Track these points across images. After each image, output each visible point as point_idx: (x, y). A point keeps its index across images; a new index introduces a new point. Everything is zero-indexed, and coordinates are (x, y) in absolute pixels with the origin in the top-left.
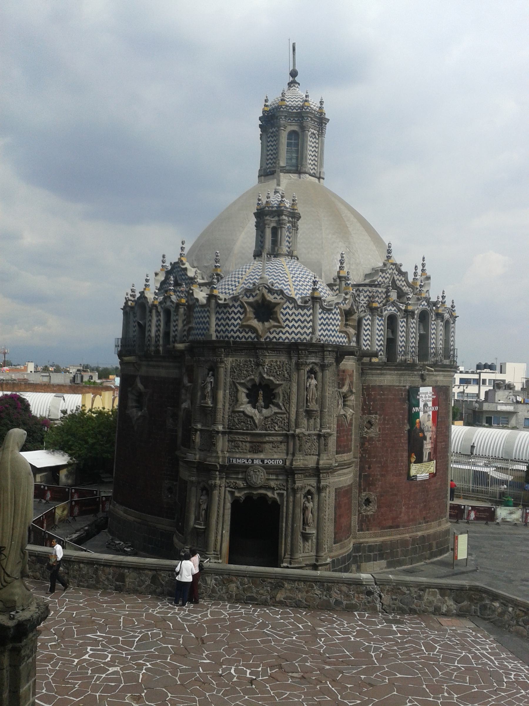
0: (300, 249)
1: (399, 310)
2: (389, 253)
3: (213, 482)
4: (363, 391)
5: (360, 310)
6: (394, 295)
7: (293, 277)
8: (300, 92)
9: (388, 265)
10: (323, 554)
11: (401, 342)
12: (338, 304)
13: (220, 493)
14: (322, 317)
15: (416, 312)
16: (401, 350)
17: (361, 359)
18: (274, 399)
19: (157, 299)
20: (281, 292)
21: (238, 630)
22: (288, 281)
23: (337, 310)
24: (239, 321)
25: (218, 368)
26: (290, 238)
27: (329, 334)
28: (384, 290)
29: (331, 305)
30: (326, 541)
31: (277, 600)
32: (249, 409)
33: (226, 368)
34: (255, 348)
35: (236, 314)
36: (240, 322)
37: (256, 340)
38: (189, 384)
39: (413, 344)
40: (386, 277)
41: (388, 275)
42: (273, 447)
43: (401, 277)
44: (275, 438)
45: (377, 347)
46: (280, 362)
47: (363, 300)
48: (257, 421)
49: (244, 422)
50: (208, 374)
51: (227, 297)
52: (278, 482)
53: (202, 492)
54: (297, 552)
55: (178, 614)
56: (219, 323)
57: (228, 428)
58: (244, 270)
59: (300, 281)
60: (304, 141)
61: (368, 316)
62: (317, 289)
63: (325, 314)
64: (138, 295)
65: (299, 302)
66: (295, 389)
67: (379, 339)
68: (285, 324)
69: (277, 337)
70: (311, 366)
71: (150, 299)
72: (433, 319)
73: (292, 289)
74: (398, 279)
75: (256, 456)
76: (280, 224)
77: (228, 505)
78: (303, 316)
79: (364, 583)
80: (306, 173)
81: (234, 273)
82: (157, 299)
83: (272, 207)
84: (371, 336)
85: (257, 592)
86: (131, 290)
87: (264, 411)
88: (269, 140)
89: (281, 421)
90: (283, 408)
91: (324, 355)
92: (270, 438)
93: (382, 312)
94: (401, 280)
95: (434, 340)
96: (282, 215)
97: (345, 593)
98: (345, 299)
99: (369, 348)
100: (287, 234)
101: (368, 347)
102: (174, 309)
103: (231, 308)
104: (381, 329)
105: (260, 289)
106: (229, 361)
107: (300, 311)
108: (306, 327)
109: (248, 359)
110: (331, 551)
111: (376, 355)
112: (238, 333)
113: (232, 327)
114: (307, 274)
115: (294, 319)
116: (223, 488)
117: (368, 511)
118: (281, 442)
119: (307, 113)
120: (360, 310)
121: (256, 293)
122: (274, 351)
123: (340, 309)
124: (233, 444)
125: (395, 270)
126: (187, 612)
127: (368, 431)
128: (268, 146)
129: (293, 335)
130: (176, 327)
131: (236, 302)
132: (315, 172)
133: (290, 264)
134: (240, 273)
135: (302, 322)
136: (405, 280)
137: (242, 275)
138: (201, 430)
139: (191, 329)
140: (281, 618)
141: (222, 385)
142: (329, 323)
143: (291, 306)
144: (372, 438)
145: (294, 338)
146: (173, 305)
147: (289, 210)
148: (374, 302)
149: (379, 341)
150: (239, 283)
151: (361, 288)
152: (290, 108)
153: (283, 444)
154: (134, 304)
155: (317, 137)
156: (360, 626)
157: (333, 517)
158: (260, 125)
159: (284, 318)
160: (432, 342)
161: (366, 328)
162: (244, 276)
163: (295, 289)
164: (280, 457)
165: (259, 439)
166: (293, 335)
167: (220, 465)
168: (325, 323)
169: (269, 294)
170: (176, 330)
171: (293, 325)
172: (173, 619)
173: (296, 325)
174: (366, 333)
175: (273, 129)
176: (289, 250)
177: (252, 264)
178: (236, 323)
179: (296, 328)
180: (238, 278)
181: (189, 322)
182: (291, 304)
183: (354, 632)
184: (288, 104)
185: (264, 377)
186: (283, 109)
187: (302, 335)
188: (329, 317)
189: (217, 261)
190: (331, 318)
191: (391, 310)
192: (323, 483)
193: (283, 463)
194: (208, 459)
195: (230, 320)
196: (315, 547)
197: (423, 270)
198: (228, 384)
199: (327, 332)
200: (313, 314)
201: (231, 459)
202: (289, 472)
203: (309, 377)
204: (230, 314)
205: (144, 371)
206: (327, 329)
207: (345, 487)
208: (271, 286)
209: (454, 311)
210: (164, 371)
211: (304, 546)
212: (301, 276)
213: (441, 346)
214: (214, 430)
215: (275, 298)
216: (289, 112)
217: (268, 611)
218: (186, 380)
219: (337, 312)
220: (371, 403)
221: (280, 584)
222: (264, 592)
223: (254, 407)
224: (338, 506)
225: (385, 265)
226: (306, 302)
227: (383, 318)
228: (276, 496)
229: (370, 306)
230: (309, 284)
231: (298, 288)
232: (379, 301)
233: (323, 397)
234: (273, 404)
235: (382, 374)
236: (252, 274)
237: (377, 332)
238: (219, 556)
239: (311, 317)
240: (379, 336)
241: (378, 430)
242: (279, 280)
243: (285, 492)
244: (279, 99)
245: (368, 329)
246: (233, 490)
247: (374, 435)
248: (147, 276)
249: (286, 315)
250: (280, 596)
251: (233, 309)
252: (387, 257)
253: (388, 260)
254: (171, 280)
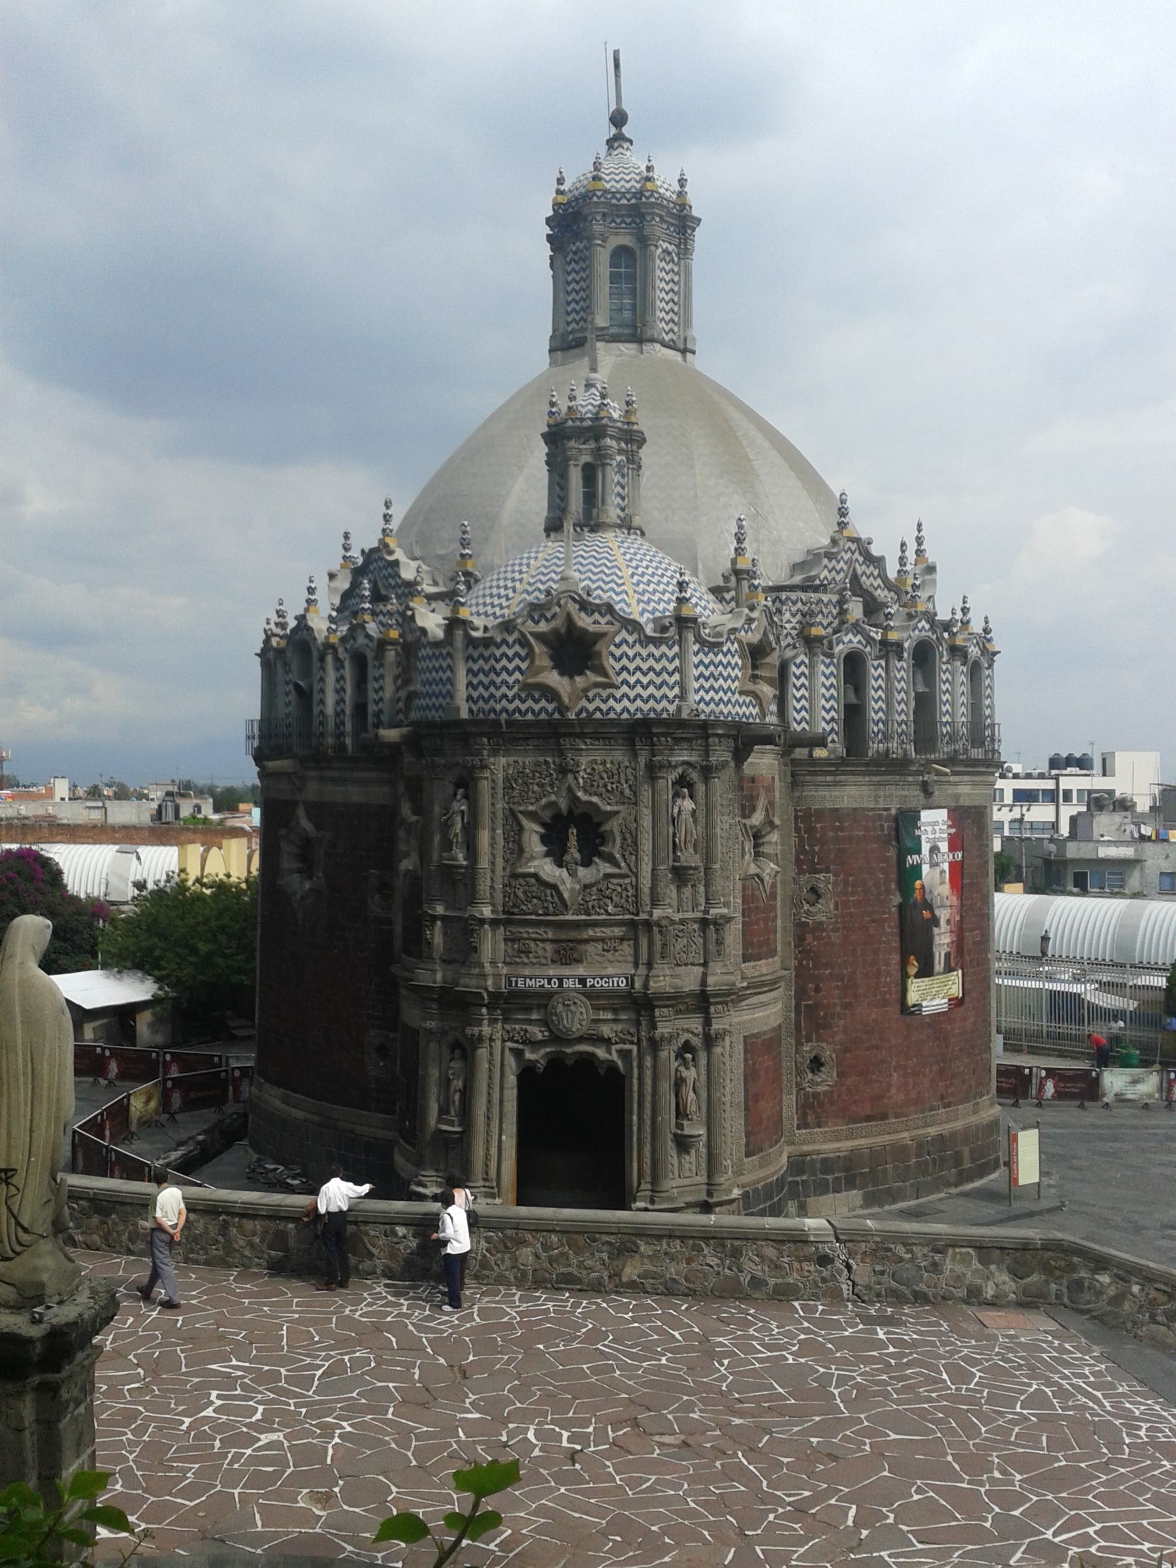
0: (648, 511)
1: (870, 640)
2: (843, 515)
3: (476, 1030)
4: (796, 823)
5: (783, 644)
6: (856, 610)
7: (633, 575)
8: (635, 159)
9: (841, 543)
10: (722, 1180)
11: (876, 713)
12: (734, 630)
13: (491, 1054)
14: (701, 662)
15: (906, 645)
16: (876, 729)
17: (791, 753)
18: (602, 844)
19: (335, 631)
20: (609, 609)
21: (541, 1347)
22: (623, 584)
23: (733, 643)
24: (517, 675)
25: (476, 780)
26: (623, 487)
27: (717, 698)
28: (835, 598)
29: (720, 635)
30: (729, 1151)
31: (624, 1279)
32: (548, 869)
33: (493, 781)
34: (556, 734)
35: (510, 660)
36: (520, 678)
37: (556, 716)
38: (414, 818)
39: (903, 717)
40: (838, 568)
41: (842, 563)
42: (604, 950)
43: (871, 568)
44: (608, 932)
45: (824, 724)
46: (612, 762)
47: (790, 621)
48: (566, 895)
49: (539, 899)
50: (455, 794)
51: (491, 622)
52: (619, 1027)
53: (452, 1052)
54: (666, 1177)
55: (408, 1316)
56: (475, 681)
57: (504, 912)
58: (525, 561)
59: (649, 583)
60: (647, 272)
61: (802, 657)
62: (688, 600)
63: (706, 654)
64: (292, 624)
65: (649, 630)
66: (646, 822)
67: (828, 706)
68: (620, 679)
69: (604, 707)
70: (680, 770)
71: (320, 631)
72: (944, 660)
73: (634, 602)
74: (864, 573)
75: (566, 971)
76: (601, 455)
77: (512, 1080)
78: (658, 660)
79: (812, 1239)
80: (652, 340)
81: (503, 569)
82: (335, 631)
83: (582, 420)
84: (810, 700)
85: (581, 1265)
86: (277, 612)
87: (582, 871)
88: (569, 269)
89: (620, 894)
90: (623, 864)
91: (707, 746)
92: (597, 930)
93: (831, 648)
94: (872, 574)
95: (948, 706)
96: (605, 436)
97: (771, 1261)
98: (750, 620)
99: (807, 728)
100: (617, 478)
101: (804, 724)
102: (373, 654)
103: (498, 646)
104: (832, 685)
105: (562, 602)
106: (500, 765)
107: (652, 648)
108: (667, 684)
109: (541, 759)
110: (739, 1172)
111: (821, 742)
112: (517, 702)
113: (504, 689)
114: (663, 566)
115: (638, 668)
116: (499, 1043)
117: (818, 1084)
118: (622, 939)
119: (653, 205)
120: (783, 644)
121: (553, 612)
122: (598, 739)
123: (740, 642)
124: (516, 946)
125: (857, 554)
126: (428, 1312)
127: (811, 909)
128: (568, 283)
129: (639, 703)
130: (381, 693)
131: (510, 633)
132: (675, 338)
133: (626, 545)
134: (517, 568)
135: (658, 674)
136: (879, 575)
137: (521, 572)
138: (444, 918)
139: (412, 696)
140: (634, 1320)
141: (485, 818)
142: (716, 674)
143: (631, 639)
144: (821, 923)
145: (642, 710)
146: (370, 644)
147: (619, 424)
148: (813, 625)
149: (828, 711)
150: (514, 591)
151: (784, 595)
152: (614, 197)
153: (625, 943)
154: (283, 643)
155: (676, 259)
156: (806, 1331)
157: (741, 1098)
158: (548, 236)
159: (618, 666)
160: (944, 710)
161: (798, 684)
162: (524, 576)
163: (639, 601)
164: (620, 972)
165: (573, 935)
166: (639, 703)
167: (489, 993)
168: (707, 674)
169: (583, 614)
170: (381, 699)
171: (638, 681)
172: (398, 1328)
173: (645, 680)
174: (798, 695)
175: (578, 244)
176: (622, 515)
177: (541, 549)
178: (511, 680)
179: (645, 687)
180: (513, 580)
181: (408, 681)
182: (631, 634)
183: (794, 1345)
184: (608, 186)
185: (578, 798)
186: (599, 197)
187: (658, 701)
188: (717, 661)
189: (464, 544)
190: (721, 662)
191: (850, 641)
192: (716, 1026)
193: (627, 985)
194: (462, 981)
195: (498, 675)
196: (704, 1165)
197: (919, 552)
198: (500, 814)
199: (712, 693)
200: (680, 656)
202: (640, 1005)
203: (676, 795)
204: (497, 661)
205: (313, 791)
206: (712, 687)
207: (765, 1033)
208: (585, 596)
209: (989, 640)
210: (358, 791)
211: (680, 1163)
212: (650, 571)
213: (964, 719)
214: (473, 918)
215: (596, 622)
216: (612, 205)
217: (604, 1305)
218: (406, 810)
219: (733, 650)
220: (817, 849)
221: (629, 1245)
222: (595, 1264)
223: (560, 864)
224: (751, 1075)
225: (834, 542)
226: (664, 629)
227: (835, 661)
228: (615, 1057)
229: (806, 633)
230: (670, 588)
231: (645, 598)
232: (825, 623)
233: (709, 838)
234: (601, 855)
235: (836, 784)
236: (543, 569)
237: (823, 690)
238: (496, 1190)
239: (677, 662)
240: (827, 701)
241: (832, 907)
242: (604, 582)
243: (635, 1048)
244: (589, 175)
245: (803, 685)
246: (520, 1046)
247: (824, 919)
248: (311, 581)
249: (620, 659)
250: (631, 1272)
251: (504, 648)
252: (839, 524)
253: (840, 531)
254: (365, 589)
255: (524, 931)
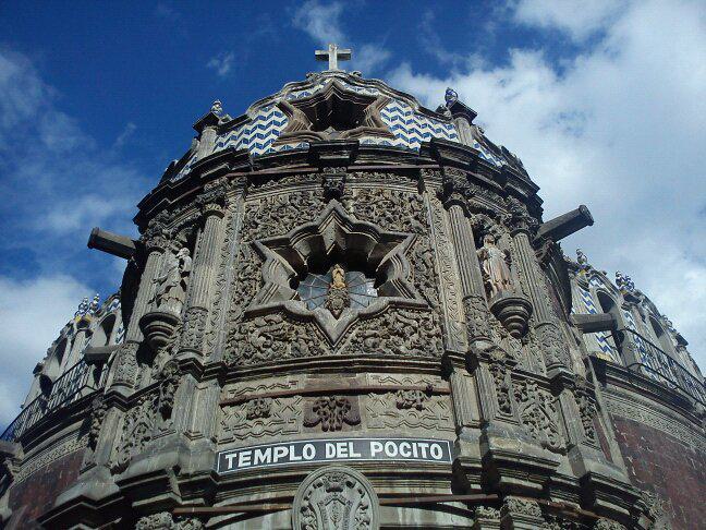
42: (400, 406)
159: (391, 124)
165: (344, 381)
185: (345, 221)
193: (445, 457)
201: (230, 457)
255: (255, 387)
